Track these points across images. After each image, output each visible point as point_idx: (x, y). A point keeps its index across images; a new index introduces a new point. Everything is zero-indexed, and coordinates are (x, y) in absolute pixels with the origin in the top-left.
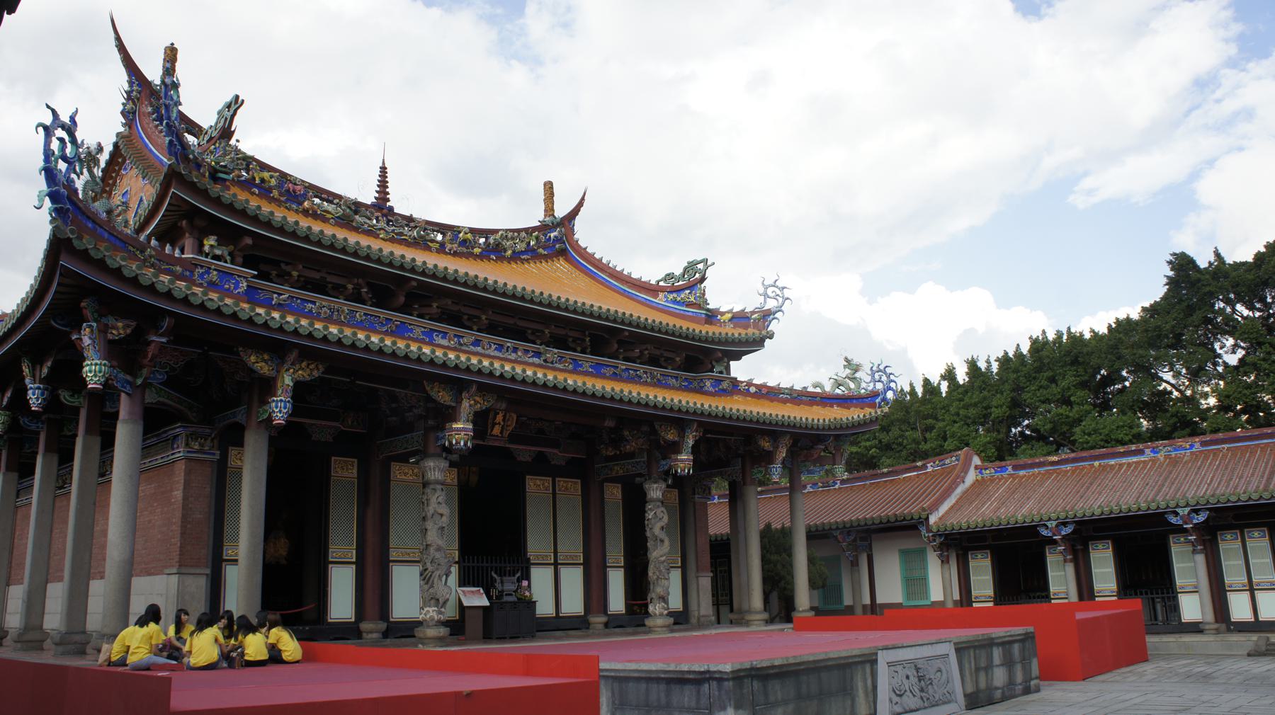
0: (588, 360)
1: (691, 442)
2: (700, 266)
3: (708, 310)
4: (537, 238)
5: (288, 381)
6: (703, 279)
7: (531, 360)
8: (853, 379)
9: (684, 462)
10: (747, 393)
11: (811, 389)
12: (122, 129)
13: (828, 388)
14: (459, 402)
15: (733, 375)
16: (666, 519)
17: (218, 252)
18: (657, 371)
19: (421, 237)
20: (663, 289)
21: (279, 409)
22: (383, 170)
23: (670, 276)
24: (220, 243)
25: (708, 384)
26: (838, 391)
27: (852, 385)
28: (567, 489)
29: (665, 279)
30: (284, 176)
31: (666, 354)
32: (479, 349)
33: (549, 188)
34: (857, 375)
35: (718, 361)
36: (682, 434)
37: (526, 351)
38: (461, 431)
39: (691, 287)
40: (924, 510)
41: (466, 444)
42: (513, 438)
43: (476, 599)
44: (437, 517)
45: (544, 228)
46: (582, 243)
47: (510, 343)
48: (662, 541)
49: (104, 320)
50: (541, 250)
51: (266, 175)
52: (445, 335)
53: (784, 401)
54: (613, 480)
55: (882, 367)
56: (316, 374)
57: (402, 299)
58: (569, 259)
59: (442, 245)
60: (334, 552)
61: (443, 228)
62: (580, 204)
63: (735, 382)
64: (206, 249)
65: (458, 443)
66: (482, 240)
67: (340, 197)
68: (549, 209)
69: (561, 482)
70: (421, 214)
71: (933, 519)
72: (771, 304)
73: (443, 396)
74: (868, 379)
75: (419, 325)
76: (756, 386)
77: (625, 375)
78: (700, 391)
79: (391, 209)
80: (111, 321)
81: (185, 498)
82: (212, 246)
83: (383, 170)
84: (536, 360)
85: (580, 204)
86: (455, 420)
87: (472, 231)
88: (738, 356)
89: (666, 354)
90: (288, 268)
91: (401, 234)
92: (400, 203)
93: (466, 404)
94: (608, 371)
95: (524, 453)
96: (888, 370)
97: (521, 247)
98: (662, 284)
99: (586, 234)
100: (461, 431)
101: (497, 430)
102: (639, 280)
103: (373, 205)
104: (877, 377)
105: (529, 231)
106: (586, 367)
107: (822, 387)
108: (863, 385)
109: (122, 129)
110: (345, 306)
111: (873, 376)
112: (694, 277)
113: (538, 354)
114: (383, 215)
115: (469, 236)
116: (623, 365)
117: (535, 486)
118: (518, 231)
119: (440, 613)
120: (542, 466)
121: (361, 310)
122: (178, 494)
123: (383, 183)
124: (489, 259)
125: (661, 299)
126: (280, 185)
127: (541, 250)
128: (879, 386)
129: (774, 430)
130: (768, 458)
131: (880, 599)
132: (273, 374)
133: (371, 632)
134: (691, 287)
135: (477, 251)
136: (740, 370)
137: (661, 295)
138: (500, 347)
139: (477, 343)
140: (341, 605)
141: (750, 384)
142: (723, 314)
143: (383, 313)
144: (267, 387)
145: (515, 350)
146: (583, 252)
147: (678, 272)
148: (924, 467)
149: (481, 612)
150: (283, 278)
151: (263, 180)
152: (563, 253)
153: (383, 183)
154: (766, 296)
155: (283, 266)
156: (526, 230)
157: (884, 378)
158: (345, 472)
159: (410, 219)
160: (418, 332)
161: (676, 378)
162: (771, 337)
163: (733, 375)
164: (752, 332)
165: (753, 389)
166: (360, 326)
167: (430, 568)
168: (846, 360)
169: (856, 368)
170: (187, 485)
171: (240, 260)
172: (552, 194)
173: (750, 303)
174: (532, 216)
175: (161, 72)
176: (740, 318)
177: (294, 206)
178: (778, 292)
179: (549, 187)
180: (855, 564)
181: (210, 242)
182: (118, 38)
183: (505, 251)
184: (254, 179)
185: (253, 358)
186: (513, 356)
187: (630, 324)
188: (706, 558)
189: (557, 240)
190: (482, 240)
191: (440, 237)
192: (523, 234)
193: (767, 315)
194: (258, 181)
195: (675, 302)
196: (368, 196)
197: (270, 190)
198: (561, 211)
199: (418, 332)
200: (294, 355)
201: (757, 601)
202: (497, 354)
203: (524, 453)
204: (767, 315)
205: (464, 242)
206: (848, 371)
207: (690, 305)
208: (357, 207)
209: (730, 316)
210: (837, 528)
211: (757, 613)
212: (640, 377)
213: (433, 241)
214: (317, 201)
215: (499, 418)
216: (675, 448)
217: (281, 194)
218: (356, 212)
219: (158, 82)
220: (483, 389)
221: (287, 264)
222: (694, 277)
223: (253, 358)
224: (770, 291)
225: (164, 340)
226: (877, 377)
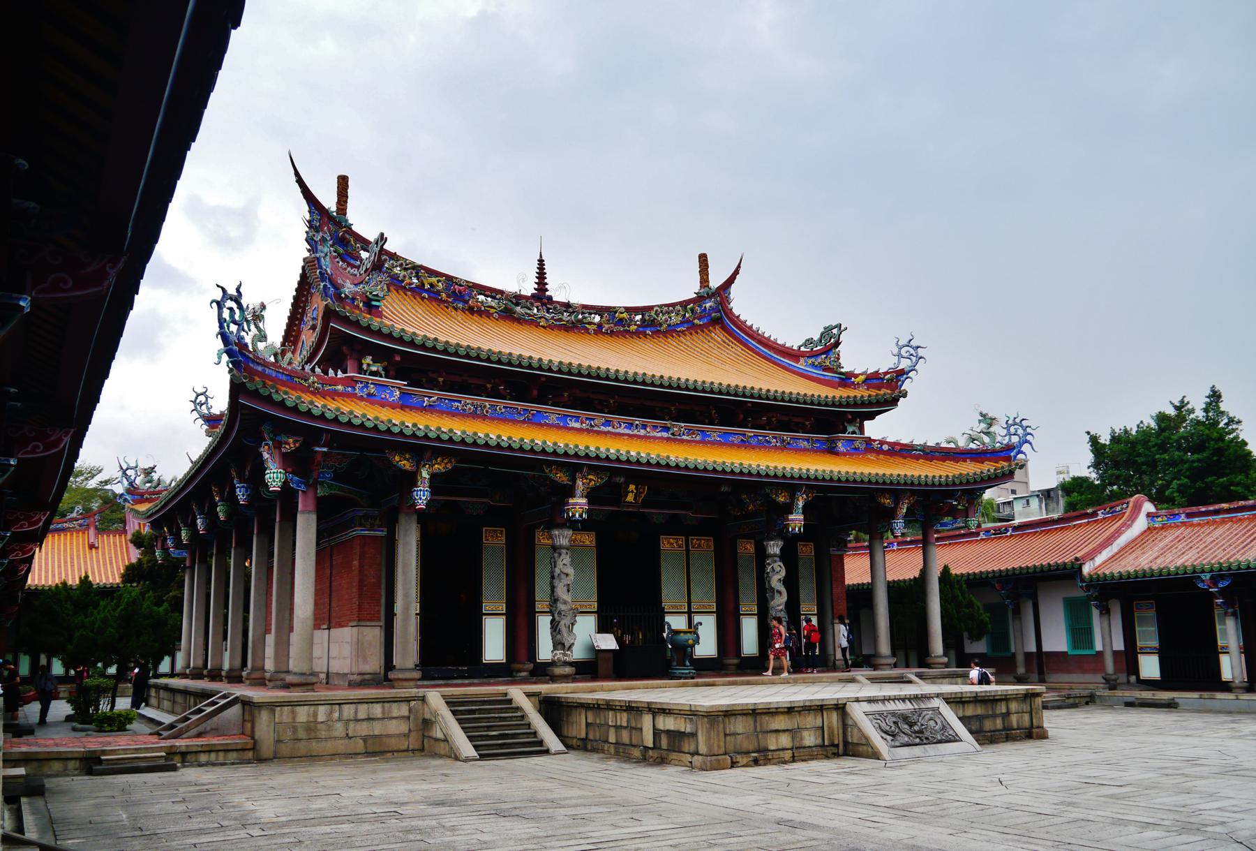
0: (715, 432)
1: (801, 504)
2: (835, 331)
3: (841, 373)
4: (692, 310)
5: (425, 474)
6: (837, 344)
7: (659, 435)
8: (987, 434)
9: (796, 520)
10: (880, 452)
11: (944, 445)
12: (307, 254)
13: (962, 443)
14: (574, 480)
15: (867, 434)
16: (783, 573)
17: (374, 369)
18: (787, 435)
19: (579, 321)
20: (803, 355)
21: (422, 496)
22: (541, 262)
23: (809, 342)
24: (374, 361)
25: (840, 444)
26: (973, 446)
27: (986, 439)
28: (699, 545)
29: (805, 345)
30: (450, 279)
31: (796, 419)
32: (610, 429)
33: (703, 259)
34: (992, 429)
35: (851, 422)
36: (793, 498)
37: (655, 427)
38: (578, 505)
39: (827, 351)
40: (1077, 559)
41: (581, 516)
42: (645, 504)
43: (608, 642)
44: (563, 576)
45: (699, 299)
46: (736, 312)
47: (638, 421)
48: (780, 592)
49: (278, 438)
50: (696, 321)
51: (434, 280)
52: (577, 418)
53: (917, 458)
54: (748, 537)
55: (1018, 421)
56: (449, 466)
57: (535, 392)
58: (725, 329)
59: (600, 325)
60: (486, 607)
61: (600, 310)
62: (736, 272)
63: (869, 441)
64: (365, 367)
65: (574, 515)
66: (639, 317)
67: (502, 292)
68: (704, 280)
69: (694, 540)
70: (577, 299)
71: (1086, 569)
72: (905, 364)
73: (561, 477)
74: (1004, 432)
75: (553, 414)
76: (889, 444)
77: (754, 441)
78: (832, 451)
79: (550, 298)
80: (284, 438)
81: (361, 566)
82: (368, 365)
83: (541, 262)
84: (665, 434)
85: (736, 272)
86: (573, 496)
87: (628, 310)
88: (871, 416)
89: (796, 419)
90: (435, 376)
91: (561, 320)
92: (558, 291)
93: (579, 482)
94: (736, 439)
95: (657, 514)
96: (1024, 423)
97: (675, 319)
98: (803, 349)
99: (742, 304)
100: (578, 505)
101: (630, 498)
102: (783, 346)
103: (533, 296)
104: (1012, 430)
105: (684, 304)
106: (715, 437)
107: (956, 443)
108: (999, 439)
109: (307, 254)
110: (487, 402)
111: (1008, 428)
112: (830, 342)
113: (666, 429)
114: (543, 304)
115: (625, 315)
116: (750, 432)
117: (669, 545)
118: (673, 305)
119: (565, 655)
120: (674, 527)
121: (501, 404)
122: (356, 563)
123: (541, 275)
124: (645, 335)
125: (801, 365)
126: (447, 288)
127: (696, 321)
128: (1015, 439)
129: (897, 490)
130: (891, 514)
131: (1047, 647)
132: (414, 469)
133: (520, 671)
134: (827, 351)
135: (633, 328)
136: (877, 429)
137: (802, 360)
138: (630, 425)
140: (494, 647)
141: (882, 442)
142: (856, 376)
143: (520, 405)
144: (411, 479)
145: (644, 427)
146: (736, 320)
147: (816, 337)
148: (1095, 514)
149: (611, 655)
150: (432, 385)
151: (431, 285)
152: (717, 322)
153: (541, 275)
154: (900, 356)
155: (430, 374)
156: (681, 303)
157: (1020, 431)
158: (494, 541)
159: (567, 306)
160: (553, 419)
161: (808, 440)
162: (905, 395)
163: (867, 434)
164: (886, 390)
165: (885, 447)
166: (503, 419)
167: (557, 618)
168: (981, 414)
169: (989, 421)
170: (362, 556)
171: (392, 373)
172: (707, 265)
173: (883, 363)
174: (688, 288)
176: (873, 379)
177: (460, 305)
178: (912, 351)
179: (703, 259)
180: (1017, 612)
181: (368, 360)
183: (661, 325)
184: (423, 285)
185: (397, 458)
186: (642, 432)
187: (752, 396)
188: (842, 607)
189: (713, 309)
190: (639, 317)
191: (597, 319)
192: (678, 307)
193: (901, 374)
194: (427, 286)
195: (813, 365)
196: (529, 289)
197: (438, 293)
198: (715, 282)
200: (429, 454)
201: (884, 647)
202: (627, 431)
203: (657, 514)
204: (901, 374)
205: (621, 320)
206: (983, 426)
207: (826, 369)
208: (518, 299)
209: (862, 378)
210: (994, 577)
211: (885, 657)
212: (769, 442)
213: (590, 323)
214: (481, 298)
215: (632, 487)
216: (789, 509)
217: (448, 296)
218: (517, 304)
219: (334, 208)
220: (593, 469)
221: (433, 372)
222: (830, 342)
223: (397, 458)
224: (903, 351)
225: (325, 450)
226: (1012, 430)
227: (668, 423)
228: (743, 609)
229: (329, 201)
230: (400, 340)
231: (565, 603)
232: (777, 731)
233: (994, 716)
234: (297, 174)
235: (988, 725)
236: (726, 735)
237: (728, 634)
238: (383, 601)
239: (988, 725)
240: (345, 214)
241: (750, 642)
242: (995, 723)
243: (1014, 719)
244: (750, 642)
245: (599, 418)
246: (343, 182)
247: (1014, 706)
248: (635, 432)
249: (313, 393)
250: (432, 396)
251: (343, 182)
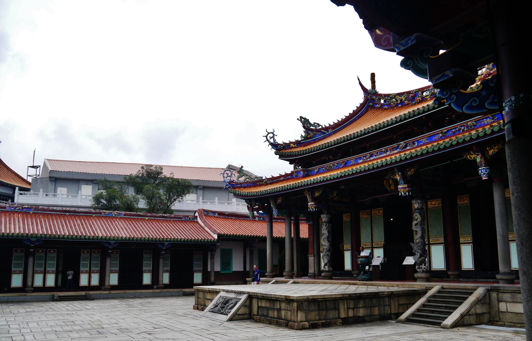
0: (423, 138)
47: (383, 149)
48: (416, 231)
52: (360, 158)
75: (351, 159)
110: (331, 164)
113: (397, 148)
116: (445, 129)
139: (371, 156)
143: (341, 161)
145: (387, 151)
160: (353, 162)
175: (371, 85)
182: (360, 84)
199: (353, 162)
212: (459, 130)
227: (395, 145)
228: (462, 240)
229: (369, 87)
230: (295, 156)
231: (325, 245)
232: (208, 299)
233: (274, 309)
234: (360, 84)
235: (271, 314)
236: (198, 298)
237: (453, 256)
238: (315, 247)
239: (271, 314)
240: (375, 88)
241: (467, 262)
242: (274, 313)
243: (283, 313)
244: (467, 262)
245: (368, 154)
246: (373, 76)
247: (283, 305)
248: (385, 155)
249: (265, 185)
250: (316, 169)
251: (373, 76)
